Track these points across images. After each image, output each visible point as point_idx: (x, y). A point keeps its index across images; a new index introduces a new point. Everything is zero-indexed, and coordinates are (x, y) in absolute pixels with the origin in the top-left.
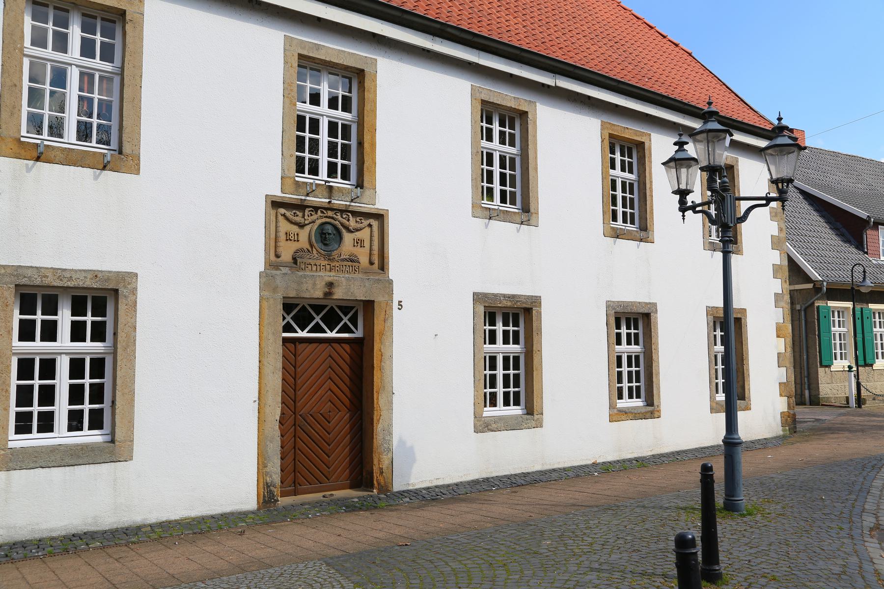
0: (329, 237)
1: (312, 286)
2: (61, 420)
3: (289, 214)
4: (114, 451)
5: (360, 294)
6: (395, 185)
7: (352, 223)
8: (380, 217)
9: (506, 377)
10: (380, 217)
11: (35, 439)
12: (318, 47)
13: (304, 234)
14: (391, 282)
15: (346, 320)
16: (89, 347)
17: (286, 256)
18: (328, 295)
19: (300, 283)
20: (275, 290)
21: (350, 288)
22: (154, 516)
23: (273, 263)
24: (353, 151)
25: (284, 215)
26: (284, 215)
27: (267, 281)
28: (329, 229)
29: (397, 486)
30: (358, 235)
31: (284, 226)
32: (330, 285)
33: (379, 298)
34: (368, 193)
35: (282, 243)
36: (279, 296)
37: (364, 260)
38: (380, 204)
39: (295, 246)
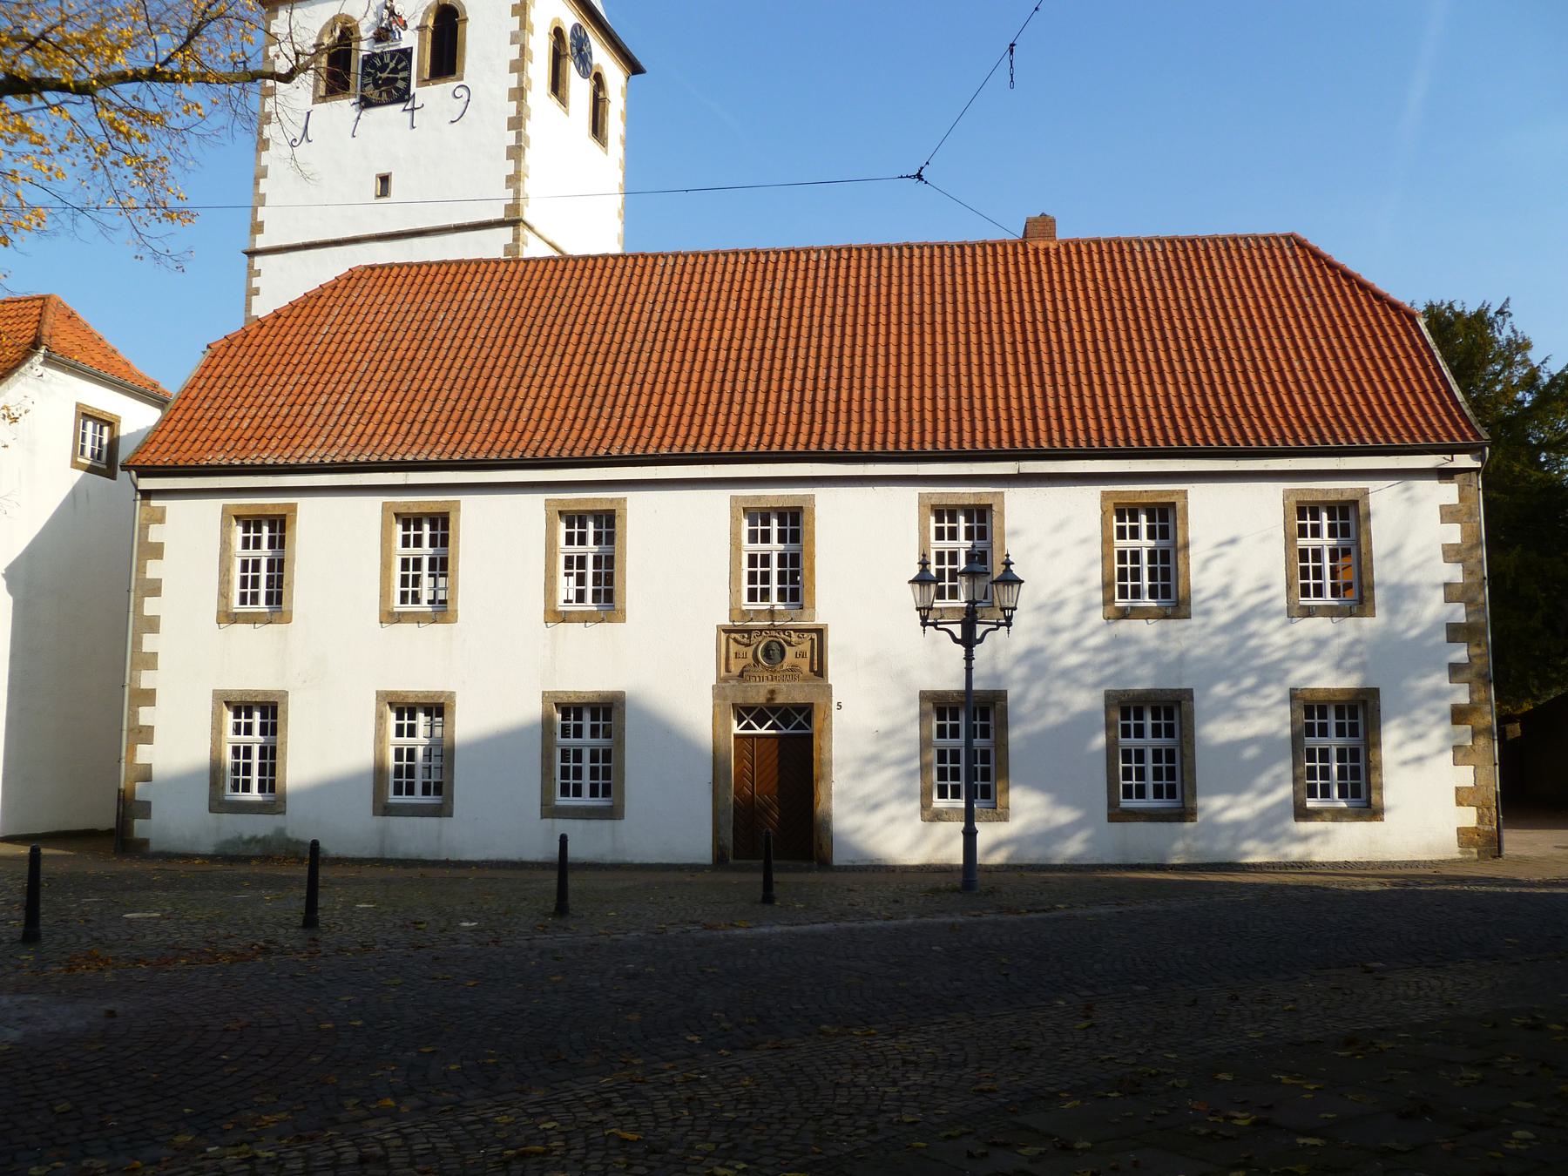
0: (774, 653)
1: (757, 693)
2: (586, 790)
3: (738, 636)
4: (613, 813)
5: (800, 698)
6: (830, 603)
7: (794, 638)
8: (820, 632)
9: (1341, 770)
10: (820, 632)
11: (571, 801)
12: (759, 498)
13: (750, 651)
14: (830, 687)
15: (800, 718)
16: (600, 742)
17: (735, 670)
18: (769, 700)
19: (745, 691)
20: (725, 699)
21: (791, 693)
22: (637, 861)
23: (720, 679)
24: (794, 579)
25: (736, 640)
26: (736, 640)
27: (718, 692)
28: (774, 646)
29: (838, 859)
30: (801, 648)
31: (734, 647)
32: (772, 692)
33: (818, 701)
34: (807, 612)
35: (732, 661)
36: (729, 703)
37: (806, 668)
38: (819, 621)
39: (743, 662)
